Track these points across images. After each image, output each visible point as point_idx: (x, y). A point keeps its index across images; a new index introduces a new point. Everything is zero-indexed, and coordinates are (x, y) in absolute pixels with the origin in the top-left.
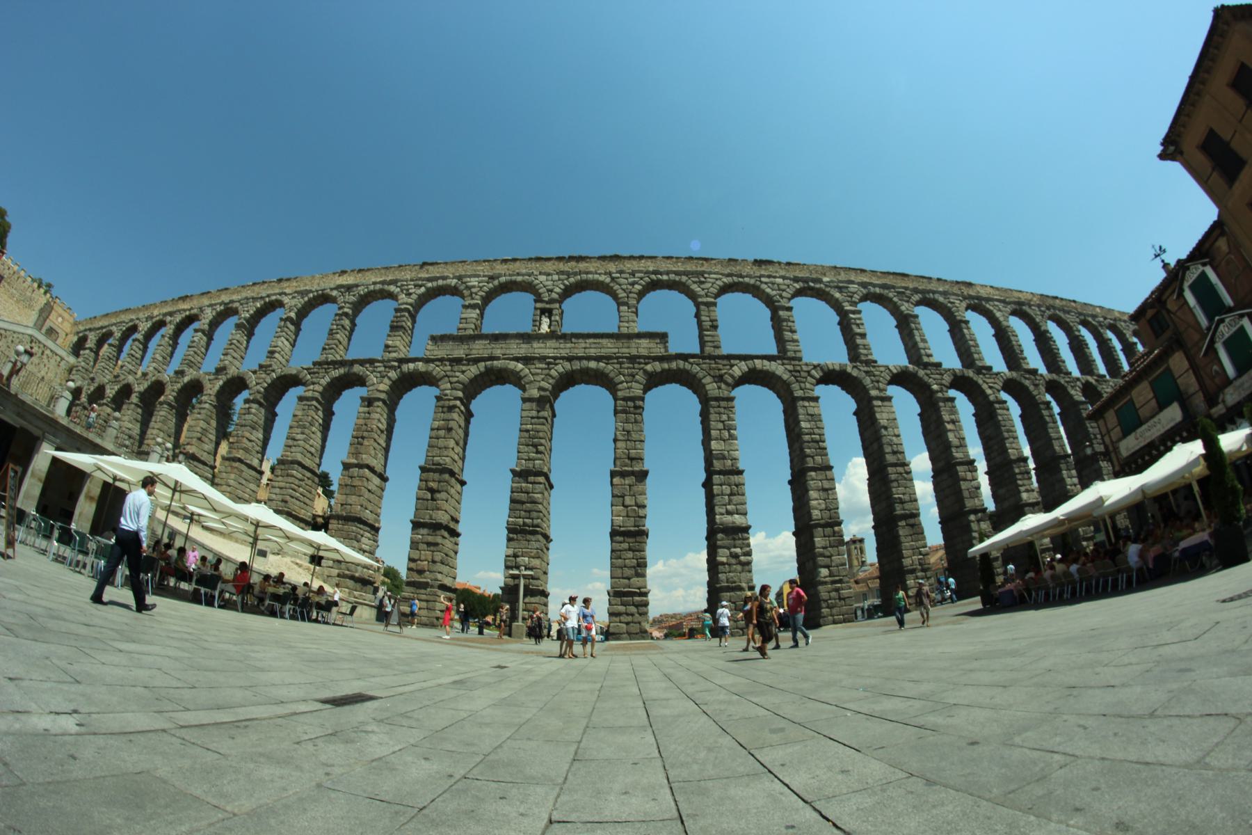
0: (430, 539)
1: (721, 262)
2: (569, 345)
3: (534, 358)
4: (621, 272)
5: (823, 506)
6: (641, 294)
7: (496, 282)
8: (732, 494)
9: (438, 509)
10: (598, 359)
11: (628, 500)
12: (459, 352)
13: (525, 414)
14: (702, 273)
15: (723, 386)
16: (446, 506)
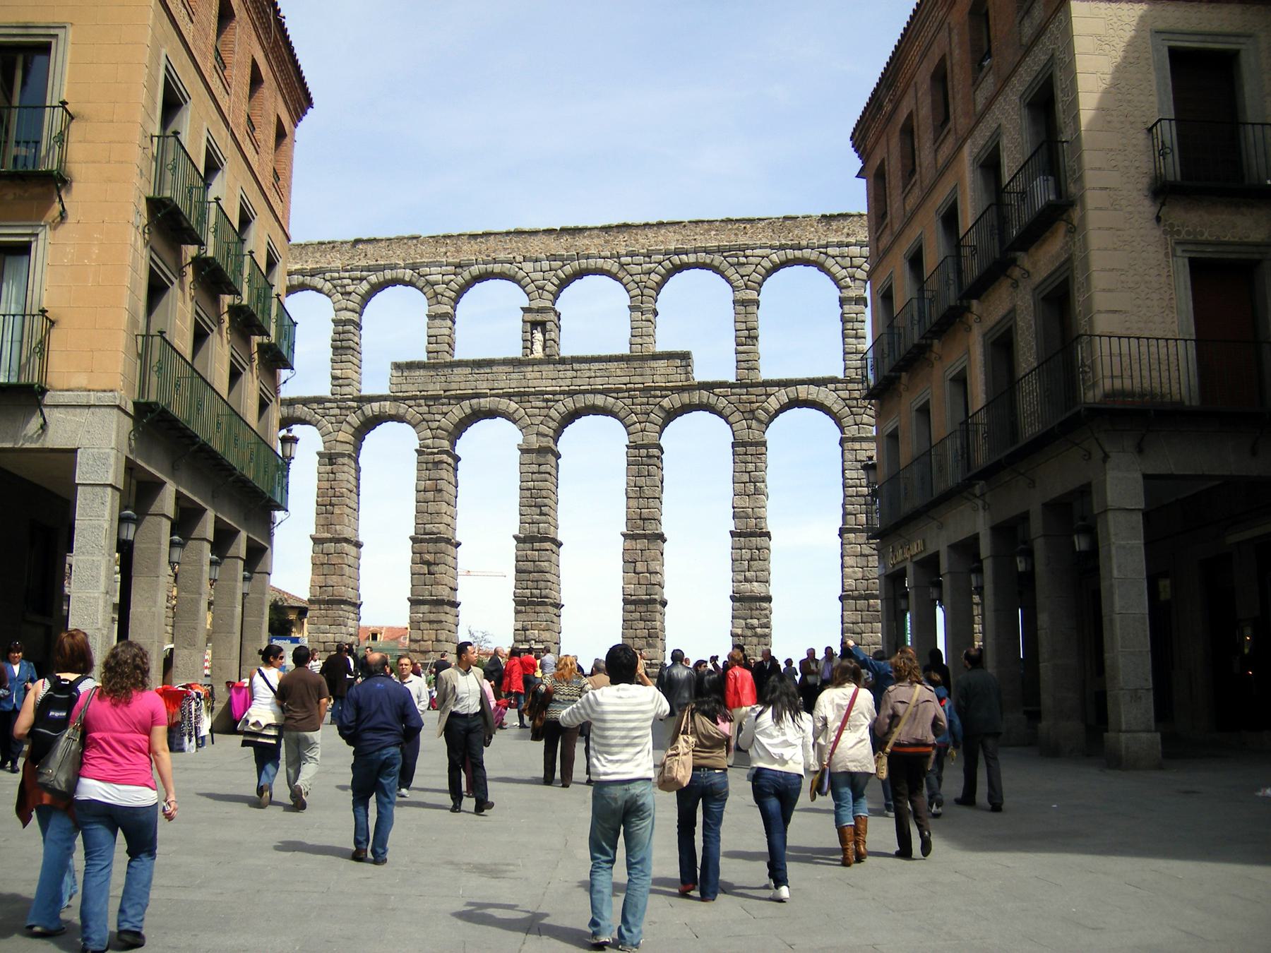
0: (432, 617)
1: (770, 222)
2: (570, 374)
3: (529, 394)
4: (632, 254)
5: (860, 575)
6: (660, 286)
7: (467, 275)
8: (752, 559)
9: (438, 584)
10: (605, 392)
11: (640, 567)
12: (435, 388)
13: (525, 468)
14: (743, 248)
15: (754, 424)
16: (447, 580)
